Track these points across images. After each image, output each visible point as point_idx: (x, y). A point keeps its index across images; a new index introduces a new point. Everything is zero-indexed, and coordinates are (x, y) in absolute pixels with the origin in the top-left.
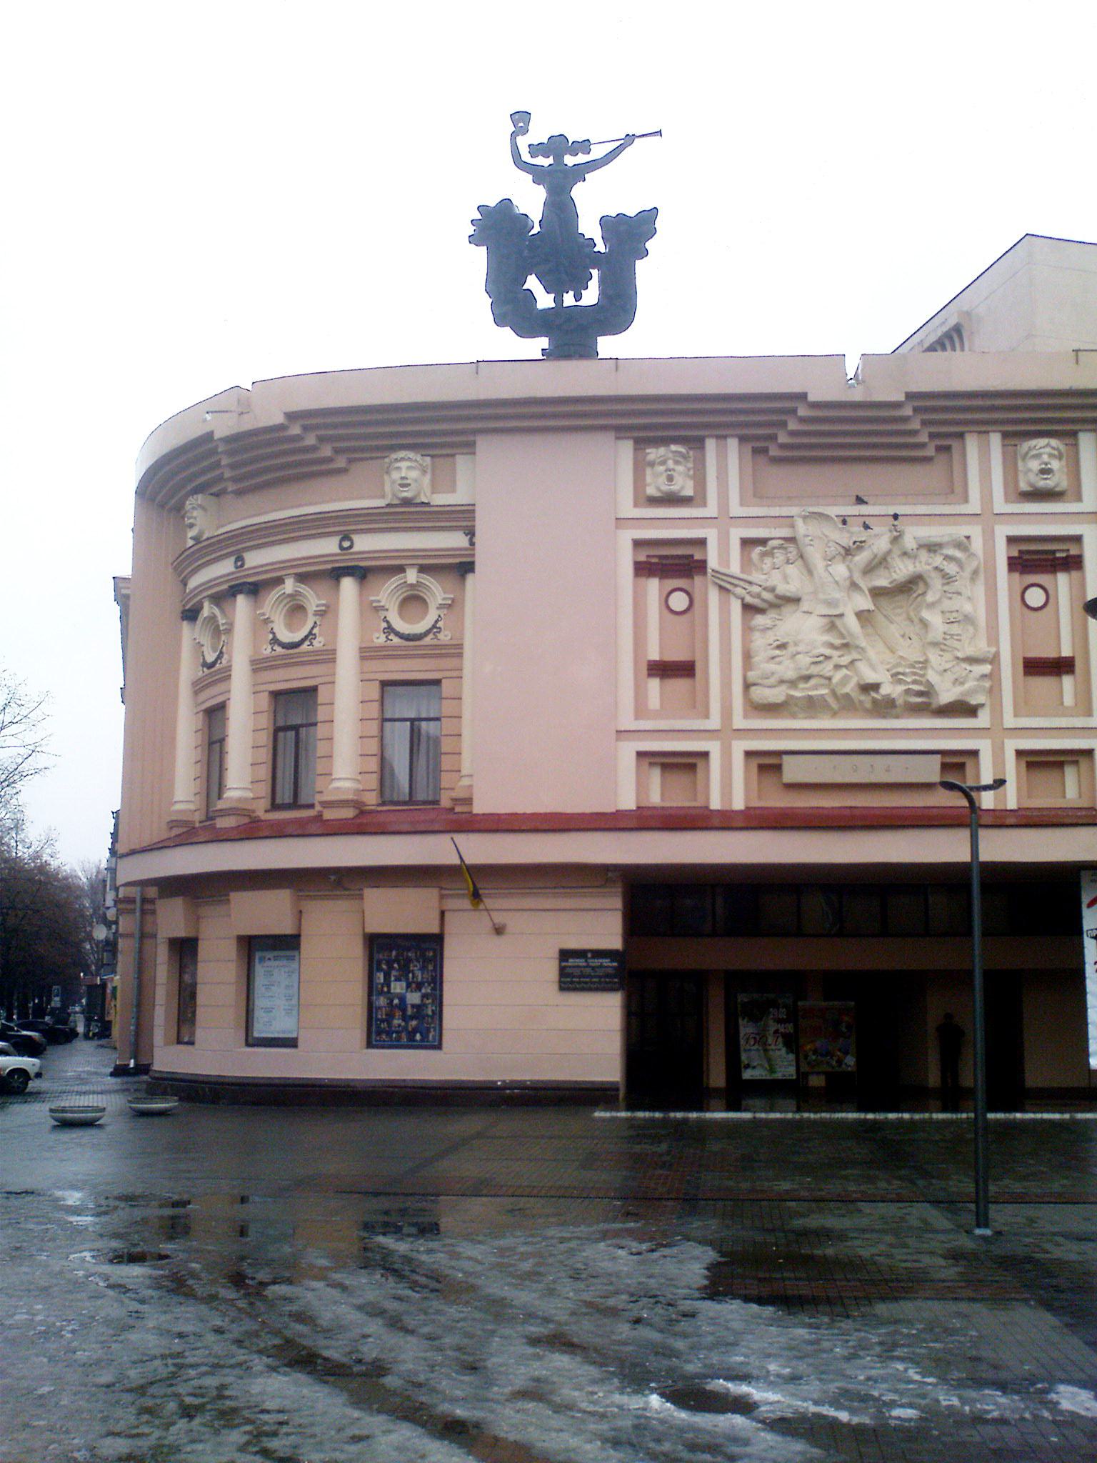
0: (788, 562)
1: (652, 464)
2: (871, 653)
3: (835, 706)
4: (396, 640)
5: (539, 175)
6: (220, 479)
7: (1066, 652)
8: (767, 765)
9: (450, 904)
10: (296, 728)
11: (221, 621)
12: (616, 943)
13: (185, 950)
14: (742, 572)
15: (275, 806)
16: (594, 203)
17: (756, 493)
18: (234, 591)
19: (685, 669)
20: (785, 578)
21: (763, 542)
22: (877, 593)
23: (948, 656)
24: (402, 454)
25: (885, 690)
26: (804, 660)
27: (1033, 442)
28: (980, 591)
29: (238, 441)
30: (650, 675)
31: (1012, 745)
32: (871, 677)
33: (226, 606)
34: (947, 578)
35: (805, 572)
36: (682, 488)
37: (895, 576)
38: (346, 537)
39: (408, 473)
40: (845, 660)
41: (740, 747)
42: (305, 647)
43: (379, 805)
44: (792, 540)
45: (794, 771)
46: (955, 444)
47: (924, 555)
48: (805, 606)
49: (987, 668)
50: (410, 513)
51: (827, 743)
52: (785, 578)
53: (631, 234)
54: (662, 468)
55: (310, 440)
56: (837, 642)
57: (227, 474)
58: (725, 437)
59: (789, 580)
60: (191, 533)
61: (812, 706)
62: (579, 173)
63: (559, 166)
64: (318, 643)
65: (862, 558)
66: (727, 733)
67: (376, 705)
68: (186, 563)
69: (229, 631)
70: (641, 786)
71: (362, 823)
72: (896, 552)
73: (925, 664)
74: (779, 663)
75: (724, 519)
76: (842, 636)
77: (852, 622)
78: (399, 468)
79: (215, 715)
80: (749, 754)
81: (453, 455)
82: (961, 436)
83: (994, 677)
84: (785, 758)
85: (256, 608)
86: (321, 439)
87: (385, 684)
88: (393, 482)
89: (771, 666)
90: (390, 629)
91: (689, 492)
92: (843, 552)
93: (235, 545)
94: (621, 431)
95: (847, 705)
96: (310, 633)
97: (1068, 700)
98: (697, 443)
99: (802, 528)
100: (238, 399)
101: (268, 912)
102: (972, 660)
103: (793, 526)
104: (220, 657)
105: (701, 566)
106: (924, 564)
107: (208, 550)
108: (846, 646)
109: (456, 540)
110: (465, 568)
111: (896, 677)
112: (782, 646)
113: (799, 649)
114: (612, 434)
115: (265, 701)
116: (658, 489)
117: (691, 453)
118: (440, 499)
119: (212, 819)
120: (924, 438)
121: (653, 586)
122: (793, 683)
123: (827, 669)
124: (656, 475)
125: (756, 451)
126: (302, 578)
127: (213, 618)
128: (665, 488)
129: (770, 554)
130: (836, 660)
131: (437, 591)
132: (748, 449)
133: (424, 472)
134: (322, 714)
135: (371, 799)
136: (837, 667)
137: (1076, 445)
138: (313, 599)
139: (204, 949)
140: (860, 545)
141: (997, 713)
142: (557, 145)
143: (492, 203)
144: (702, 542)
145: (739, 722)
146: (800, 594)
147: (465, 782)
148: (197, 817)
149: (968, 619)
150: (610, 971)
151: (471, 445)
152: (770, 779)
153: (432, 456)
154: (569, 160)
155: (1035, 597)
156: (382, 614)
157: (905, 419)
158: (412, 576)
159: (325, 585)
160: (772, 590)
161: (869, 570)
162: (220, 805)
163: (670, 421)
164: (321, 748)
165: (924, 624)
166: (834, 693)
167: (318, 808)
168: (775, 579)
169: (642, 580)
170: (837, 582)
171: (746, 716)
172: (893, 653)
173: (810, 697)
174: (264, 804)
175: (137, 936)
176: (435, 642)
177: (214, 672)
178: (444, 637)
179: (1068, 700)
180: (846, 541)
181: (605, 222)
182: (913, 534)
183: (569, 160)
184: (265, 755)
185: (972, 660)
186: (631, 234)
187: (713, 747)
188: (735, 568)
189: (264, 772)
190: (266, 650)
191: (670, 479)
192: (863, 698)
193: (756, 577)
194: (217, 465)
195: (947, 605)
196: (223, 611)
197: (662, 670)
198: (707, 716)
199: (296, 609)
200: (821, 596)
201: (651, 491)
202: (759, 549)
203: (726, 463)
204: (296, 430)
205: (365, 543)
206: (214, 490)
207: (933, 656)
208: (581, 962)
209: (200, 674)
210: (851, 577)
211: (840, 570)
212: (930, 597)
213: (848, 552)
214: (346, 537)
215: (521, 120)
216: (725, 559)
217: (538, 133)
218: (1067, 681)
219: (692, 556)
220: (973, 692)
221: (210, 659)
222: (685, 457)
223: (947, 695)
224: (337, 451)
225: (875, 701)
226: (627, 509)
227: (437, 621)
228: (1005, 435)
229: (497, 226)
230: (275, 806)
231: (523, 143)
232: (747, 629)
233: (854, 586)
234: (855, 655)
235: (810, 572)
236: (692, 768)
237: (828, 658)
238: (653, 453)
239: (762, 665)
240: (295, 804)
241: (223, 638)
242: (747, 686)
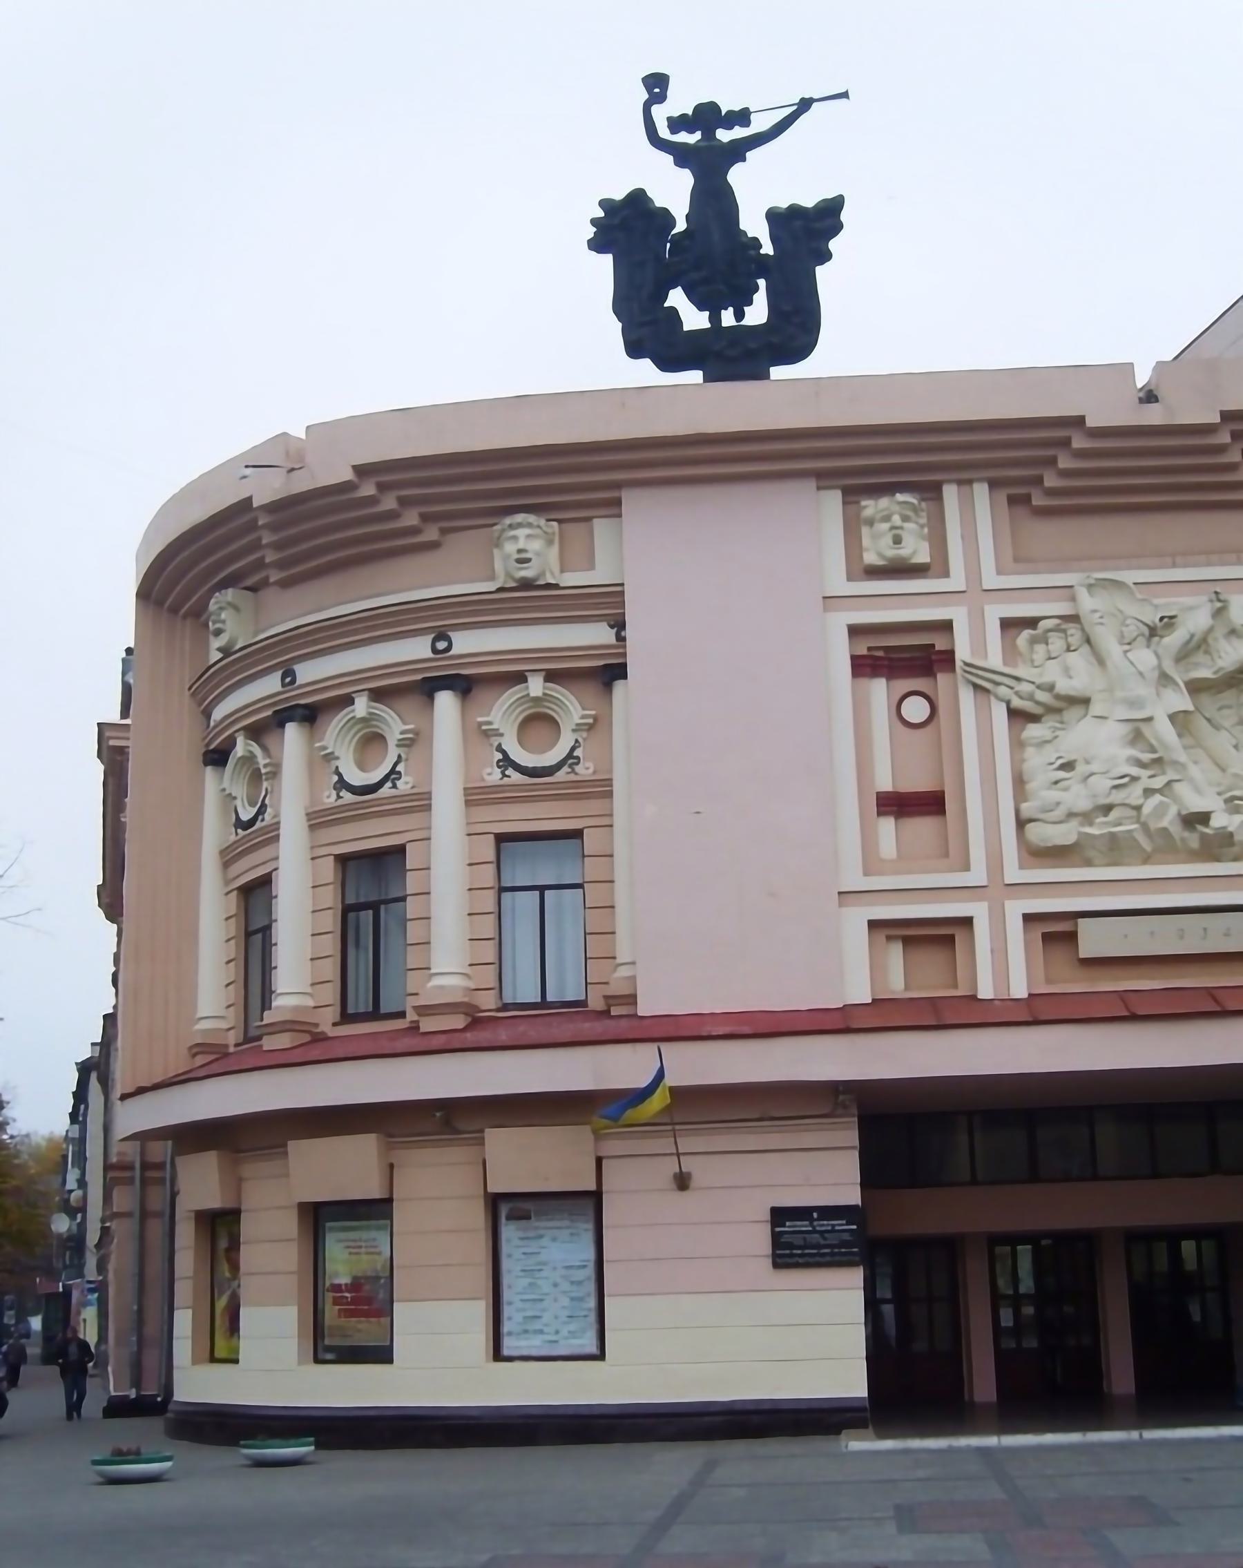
0: (1068, 650)
1: (870, 522)
2: (1194, 771)
3: (1147, 845)
4: (516, 777)
5: (682, 156)
6: (260, 565)
8: (1055, 933)
9: (611, 1147)
10: (374, 906)
11: (262, 760)
12: (853, 1196)
13: (221, 1227)
14: (1005, 664)
15: (346, 1017)
16: (761, 190)
18: (281, 718)
19: (928, 804)
20: (1067, 672)
21: (1032, 622)
22: (1196, 688)
24: (520, 518)
25: (1218, 821)
26: (1102, 784)
29: (288, 508)
30: (880, 814)
32: (1197, 804)
33: (270, 740)
35: (1096, 663)
36: (914, 553)
37: (1220, 663)
39: (529, 544)
40: (1158, 783)
41: (1015, 909)
42: (386, 791)
43: (498, 1010)
44: (1074, 618)
45: (1095, 940)
48: (1096, 708)
50: (529, 598)
52: (1067, 672)
53: (809, 231)
54: (885, 526)
55: (389, 503)
56: (1146, 757)
57: (270, 557)
58: (970, 482)
59: (1075, 674)
60: (216, 643)
61: (1116, 849)
62: (738, 151)
63: (710, 144)
65: (1174, 640)
66: (997, 889)
67: (491, 869)
68: (208, 686)
69: (275, 773)
70: (877, 969)
72: (1220, 632)
74: (1066, 789)
75: (976, 594)
76: (1154, 751)
77: (1165, 730)
78: (515, 538)
79: (255, 895)
80: (1028, 918)
81: (588, 519)
84: (1082, 922)
85: (312, 738)
86: (404, 502)
87: (501, 839)
88: (506, 557)
89: (1054, 795)
90: (507, 762)
91: (923, 556)
92: (1146, 631)
93: (282, 653)
94: (824, 478)
95: (1165, 847)
96: (393, 771)
98: (932, 492)
99: (1087, 603)
100: (282, 453)
101: (346, 1167)
103: (1073, 599)
104: (262, 810)
105: (947, 659)
107: (240, 665)
108: (1159, 761)
109: (600, 634)
113: (1094, 767)
114: (811, 484)
115: (328, 869)
116: (880, 555)
117: (924, 505)
119: (259, 1038)
121: (879, 689)
122: (1087, 817)
123: (1134, 795)
124: (876, 537)
125: (1013, 501)
126: (378, 695)
127: (250, 759)
128: (891, 553)
130: (1146, 782)
131: (572, 708)
132: (1002, 496)
133: (550, 542)
134: (412, 883)
135: (488, 1002)
136: (1148, 792)
138: (394, 725)
139: (247, 1227)
140: (1169, 622)
142: (707, 117)
143: (619, 195)
145: (1013, 873)
146: (1087, 694)
147: (623, 972)
148: (232, 1039)
150: (846, 1237)
151: (618, 503)
152: (1060, 953)
153: (559, 521)
154: (723, 135)
156: (495, 741)
157: (1221, 449)
158: (536, 686)
159: (411, 704)
160: (1050, 688)
161: (1184, 655)
162: (269, 1017)
163: (892, 460)
164: (414, 932)
166: (1145, 827)
167: (411, 1016)
169: (864, 682)
170: (1141, 674)
171: (1021, 867)
172: (1223, 770)
173: (1112, 835)
174: (332, 1014)
175: (137, 1214)
176: (572, 777)
177: (254, 832)
178: (585, 770)
180: (1152, 617)
181: (774, 217)
183: (723, 135)
184: (330, 944)
186: (809, 231)
187: (978, 910)
188: (995, 659)
189: (330, 969)
190: (329, 798)
191: (897, 540)
192: (1186, 834)
193: (1020, 672)
194: (256, 546)
196: (264, 748)
197: (897, 805)
198: (967, 867)
199: (372, 740)
200: (1119, 694)
201: (871, 558)
202: (1027, 633)
203: (973, 514)
204: (368, 490)
205: (465, 643)
206: (249, 582)
208: (803, 1226)
209: (233, 838)
210: (1160, 666)
211: (1144, 657)
213: (1153, 632)
214: (442, 635)
215: (657, 85)
216: (979, 643)
217: (680, 102)
219: (933, 646)
221: (245, 816)
222: (915, 509)
224: (425, 518)
225: (1204, 837)
226: (838, 583)
227: (573, 749)
229: (625, 226)
230: (346, 1017)
231: (661, 114)
232: (1018, 745)
233: (1164, 679)
234: (1170, 775)
235: (1101, 662)
236: (950, 940)
237: (1135, 779)
238: (871, 507)
239: (1041, 794)
240: (375, 1014)
241: (265, 784)
242: (1021, 823)
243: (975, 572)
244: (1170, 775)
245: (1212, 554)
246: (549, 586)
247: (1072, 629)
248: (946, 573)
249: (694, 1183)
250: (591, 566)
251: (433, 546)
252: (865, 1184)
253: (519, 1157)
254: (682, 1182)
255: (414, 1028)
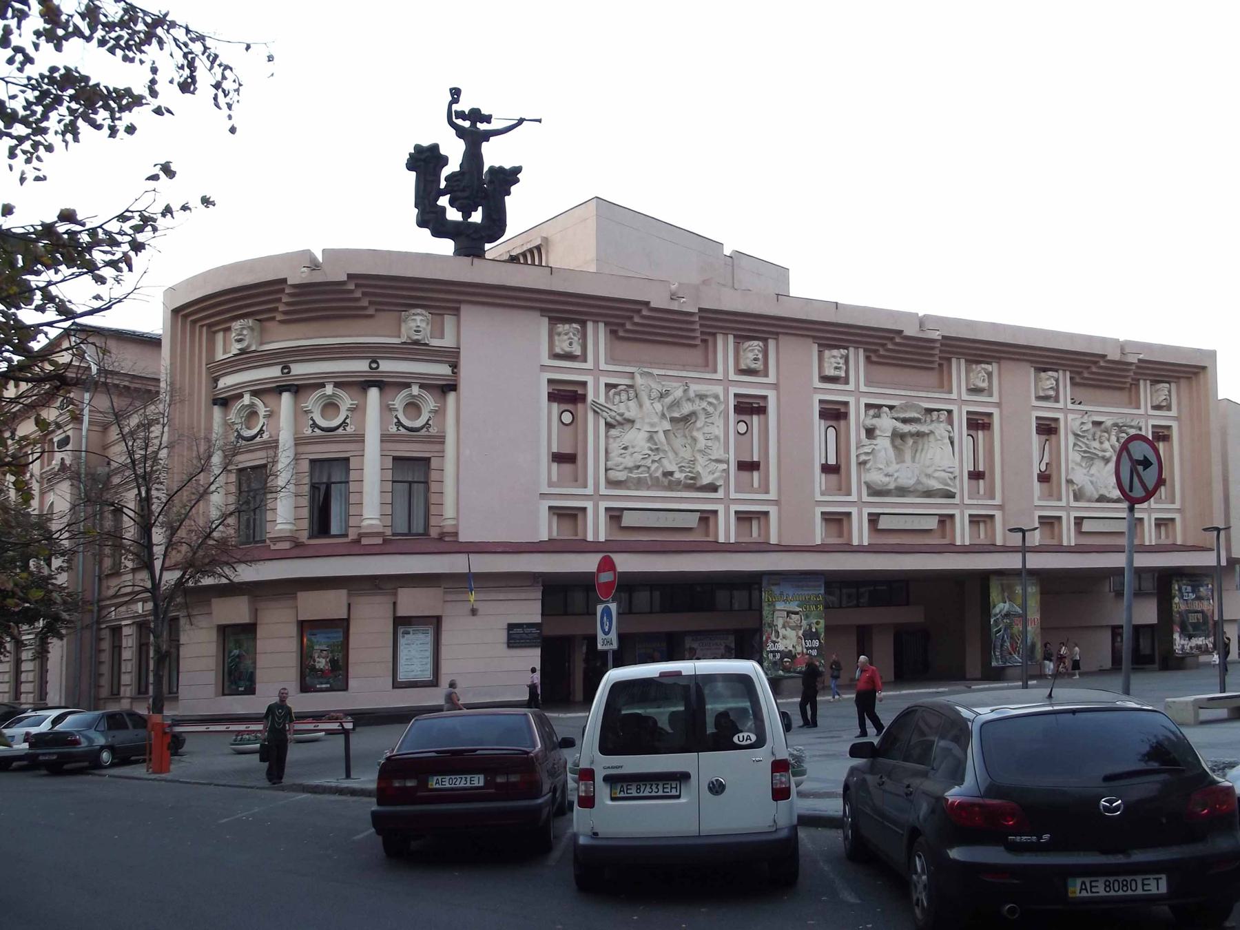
1: (559, 334)
4: (403, 431)
7: (756, 459)
8: (615, 516)
12: (537, 619)
17: (611, 359)
20: (628, 409)
21: (615, 386)
22: (673, 420)
23: (706, 458)
24: (419, 311)
25: (678, 475)
27: (751, 343)
28: (721, 423)
29: (304, 289)
31: (734, 508)
32: (670, 468)
34: (708, 415)
38: (374, 361)
39: (417, 324)
40: (657, 458)
41: (603, 505)
42: (340, 431)
45: (628, 520)
46: (710, 339)
47: (697, 401)
48: (637, 425)
49: (725, 466)
50: (414, 349)
51: (645, 504)
55: (358, 294)
59: (631, 410)
61: (639, 484)
64: (350, 429)
65: (668, 400)
66: (597, 497)
71: (388, 545)
73: (693, 461)
75: (596, 372)
77: (661, 436)
80: (607, 509)
82: (714, 335)
83: (727, 471)
89: (620, 460)
91: (578, 353)
94: (543, 311)
95: (656, 484)
96: (344, 422)
97: (756, 484)
98: (583, 323)
99: (639, 381)
101: (329, 605)
102: (718, 461)
105: (583, 398)
106: (698, 406)
109: (444, 370)
110: (447, 387)
111: (681, 469)
112: (625, 448)
114: (537, 314)
118: (435, 342)
120: (698, 334)
121: (555, 405)
122: (630, 470)
128: (568, 349)
129: (619, 394)
131: (430, 402)
134: (353, 475)
135: (388, 532)
136: (653, 461)
137: (766, 346)
138: (346, 401)
140: (668, 393)
141: (727, 492)
144: (584, 384)
145: (603, 491)
149: (717, 438)
151: (458, 309)
155: (742, 428)
158: (415, 390)
160: (622, 415)
165: (695, 440)
166: (651, 476)
168: (622, 408)
178: (433, 431)
179: (756, 484)
182: (695, 388)
185: (718, 461)
187: (589, 505)
188: (602, 400)
191: (571, 344)
194: (279, 300)
195: (706, 430)
197: (558, 458)
201: (558, 350)
203: (598, 336)
204: (351, 287)
205: (386, 366)
207: (698, 456)
208: (520, 630)
212: (699, 424)
213: (662, 396)
214: (374, 361)
218: (756, 474)
220: (716, 479)
223: (706, 480)
228: (735, 336)
232: (607, 437)
234: (662, 455)
235: (641, 406)
238: (561, 328)
239: (615, 459)
242: (606, 470)
243: (598, 361)
244: (662, 455)
245: (684, 367)
246: (426, 345)
247: (632, 392)
248: (585, 361)
249: (480, 612)
250: (442, 337)
251: (371, 316)
252: (542, 615)
253: (412, 602)
254: (474, 612)
255: (357, 541)
